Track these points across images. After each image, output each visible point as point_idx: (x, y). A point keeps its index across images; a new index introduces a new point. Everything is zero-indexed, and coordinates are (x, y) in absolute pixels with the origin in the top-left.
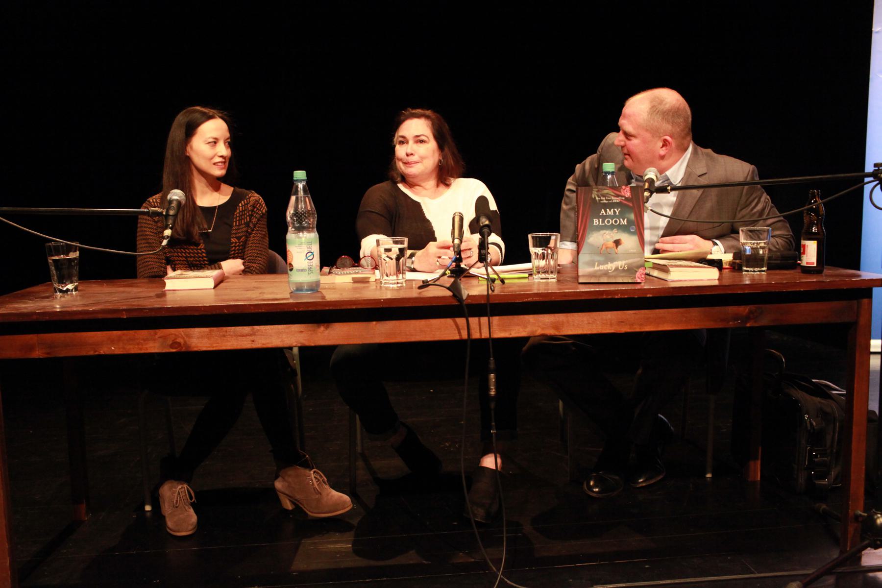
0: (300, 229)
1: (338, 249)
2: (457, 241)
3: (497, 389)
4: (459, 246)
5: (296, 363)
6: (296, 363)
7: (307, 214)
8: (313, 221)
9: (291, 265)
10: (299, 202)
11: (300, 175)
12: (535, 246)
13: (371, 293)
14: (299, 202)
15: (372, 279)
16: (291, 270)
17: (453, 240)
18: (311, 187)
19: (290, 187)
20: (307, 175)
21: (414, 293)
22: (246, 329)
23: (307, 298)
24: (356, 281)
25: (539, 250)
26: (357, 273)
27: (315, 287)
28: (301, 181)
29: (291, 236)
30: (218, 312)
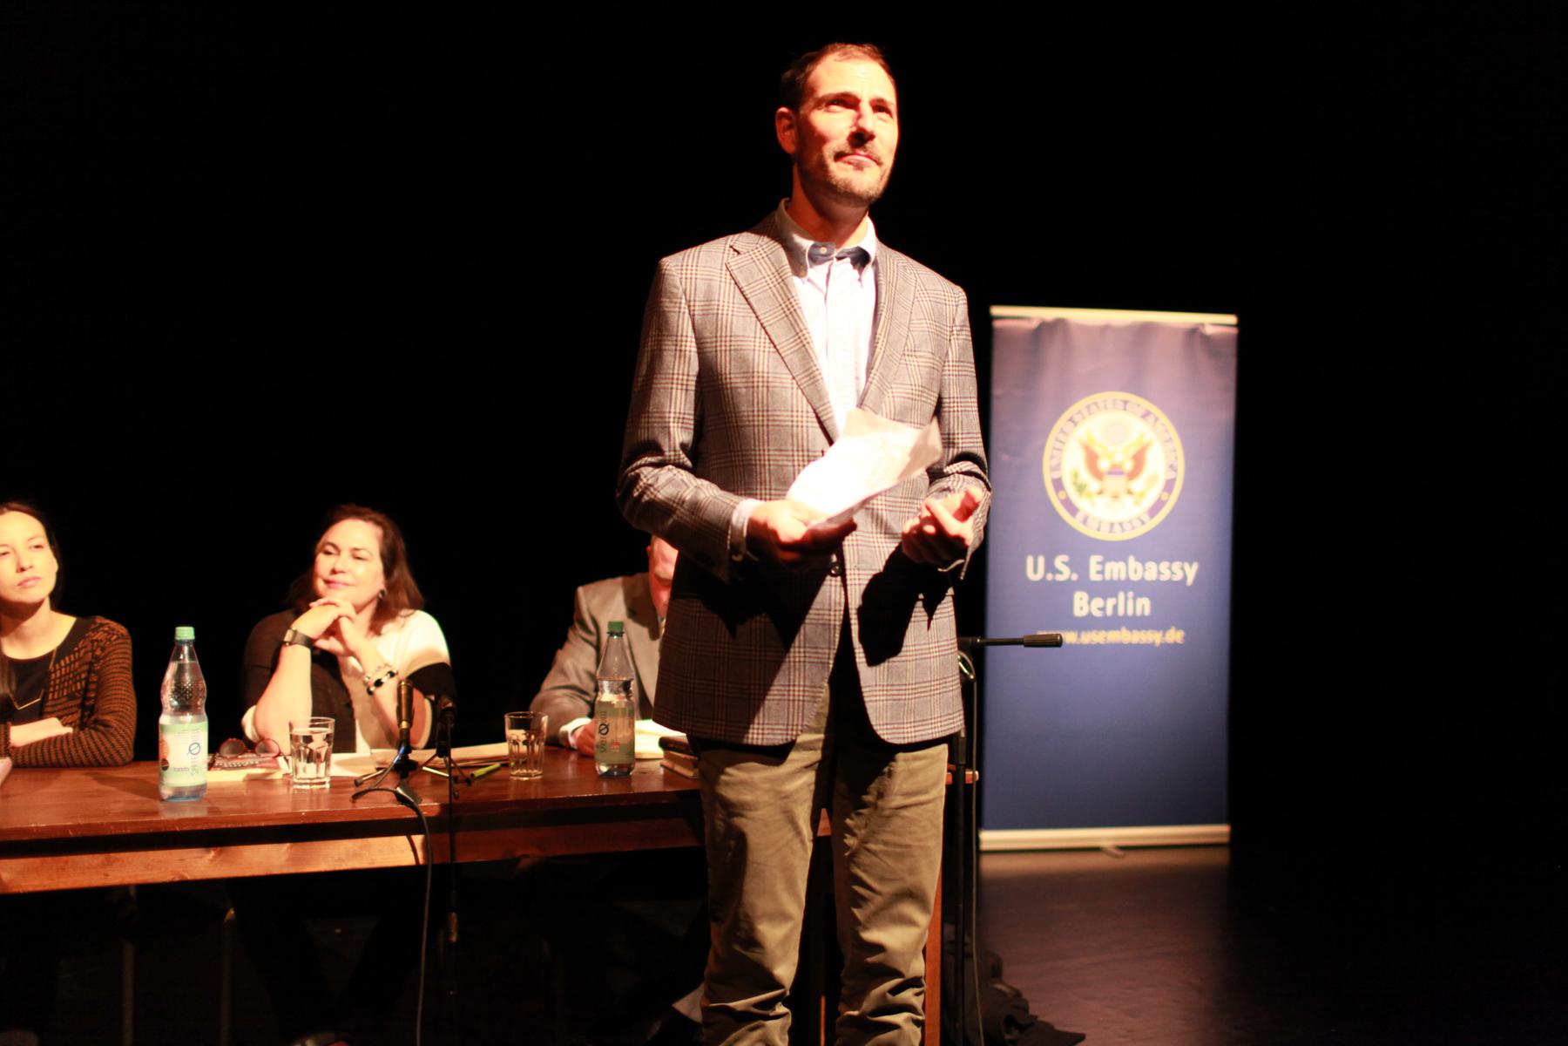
0: (185, 707)
1: (226, 734)
2: (404, 724)
3: (460, 933)
4: (408, 731)
5: (132, 892)
6: (132, 892)
7: (195, 689)
8: (201, 702)
9: (165, 761)
10: (182, 671)
11: (186, 633)
12: (513, 727)
13: (281, 805)
14: (182, 671)
15: (278, 776)
16: (165, 768)
17: (400, 722)
18: (198, 646)
19: (170, 648)
20: (196, 634)
21: (348, 806)
22: (98, 859)
23: (190, 813)
24: (252, 780)
25: (520, 734)
26: (254, 766)
27: (198, 792)
28: (188, 642)
29: (164, 719)
30: (59, 834)
